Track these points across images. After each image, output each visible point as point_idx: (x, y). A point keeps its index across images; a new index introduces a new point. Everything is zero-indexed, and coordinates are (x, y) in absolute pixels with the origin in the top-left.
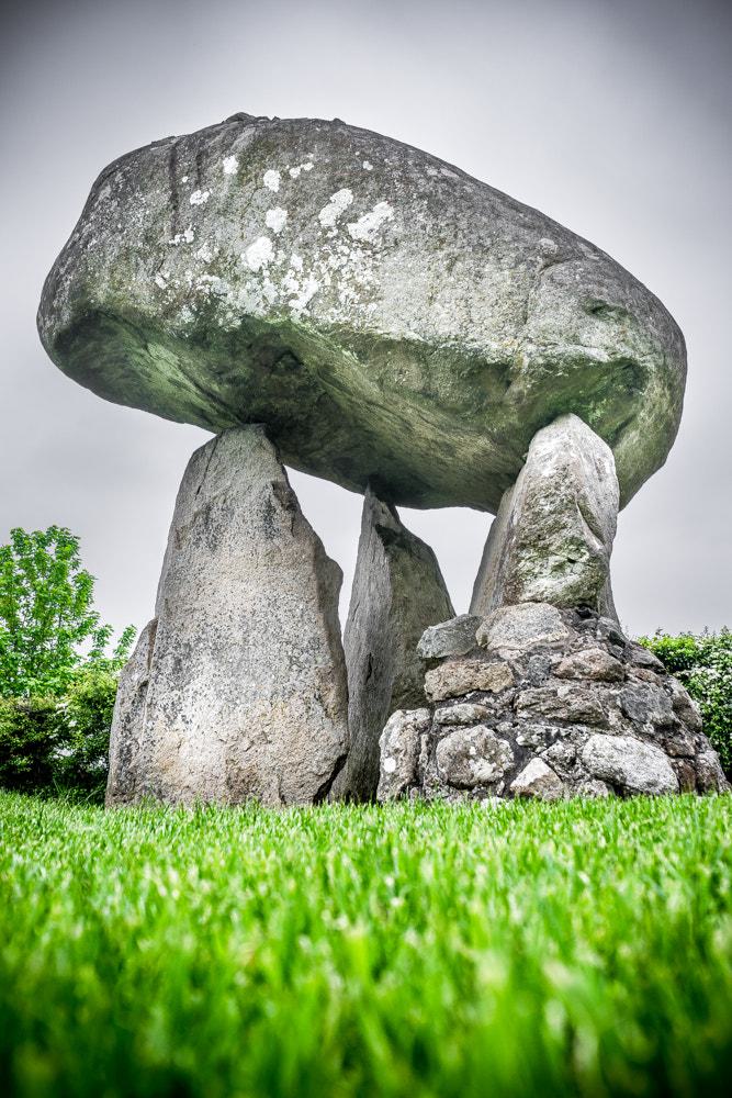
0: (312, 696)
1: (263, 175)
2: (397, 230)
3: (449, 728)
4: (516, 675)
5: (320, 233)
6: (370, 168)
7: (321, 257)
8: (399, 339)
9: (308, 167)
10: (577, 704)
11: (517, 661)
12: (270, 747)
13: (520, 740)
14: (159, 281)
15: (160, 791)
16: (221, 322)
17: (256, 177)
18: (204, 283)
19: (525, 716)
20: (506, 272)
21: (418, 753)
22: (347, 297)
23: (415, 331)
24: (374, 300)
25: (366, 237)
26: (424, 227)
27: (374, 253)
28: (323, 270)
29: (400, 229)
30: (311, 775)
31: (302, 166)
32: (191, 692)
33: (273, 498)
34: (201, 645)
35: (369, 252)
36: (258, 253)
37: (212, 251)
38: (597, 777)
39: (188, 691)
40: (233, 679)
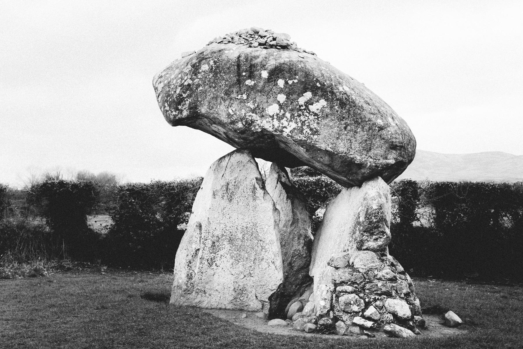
1: (278, 80)
2: (328, 110)
3: (343, 293)
4: (364, 277)
5: (298, 107)
7: (298, 116)
8: (324, 149)
9: (296, 81)
10: (384, 289)
11: (365, 273)
12: (252, 278)
13: (367, 300)
15: (205, 291)
16: (253, 129)
17: (275, 80)
18: (249, 116)
19: (368, 292)
20: (365, 132)
21: (332, 300)
22: (306, 132)
23: (330, 148)
24: (317, 135)
26: (337, 111)
27: (318, 118)
28: (298, 121)
29: (329, 111)
30: (269, 290)
31: (293, 80)
33: (256, 184)
34: (224, 237)
35: (316, 117)
36: (273, 109)
37: (254, 105)
38: (389, 313)
39: (218, 254)
40: (237, 252)
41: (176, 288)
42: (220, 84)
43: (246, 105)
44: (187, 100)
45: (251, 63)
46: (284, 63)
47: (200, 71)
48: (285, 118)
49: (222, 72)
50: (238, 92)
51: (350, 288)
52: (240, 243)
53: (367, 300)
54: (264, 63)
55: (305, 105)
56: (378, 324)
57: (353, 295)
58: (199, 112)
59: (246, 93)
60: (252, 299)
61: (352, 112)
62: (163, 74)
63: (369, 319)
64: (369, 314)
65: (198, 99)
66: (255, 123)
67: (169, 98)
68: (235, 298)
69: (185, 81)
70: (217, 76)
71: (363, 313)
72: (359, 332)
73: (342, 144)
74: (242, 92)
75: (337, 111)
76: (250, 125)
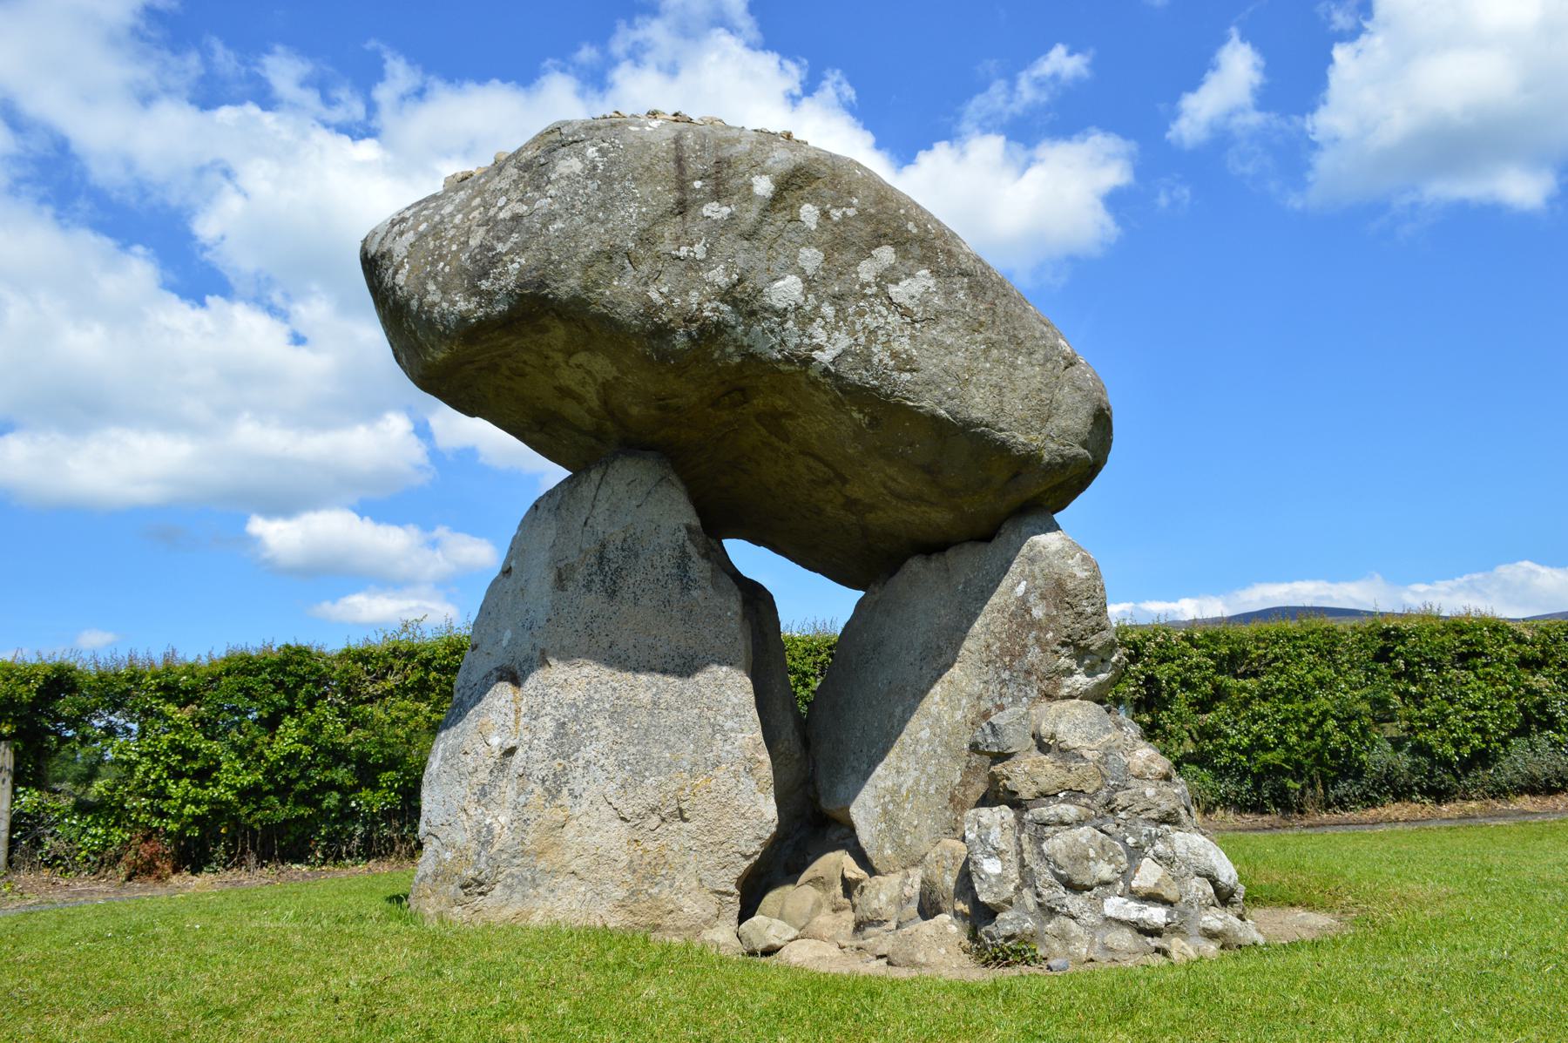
0: (742, 769)
1: (800, 207)
3: (1053, 829)
4: (1103, 776)
5: (857, 287)
6: (915, 231)
7: (856, 313)
9: (851, 212)
12: (686, 825)
13: (1131, 841)
14: (654, 296)
16: (716, 355)
18: (714, 310)
19: (1125, 817)
21: (1021, 852)
23: (946, 409)
25: (907, 302)
26: (964, 306)
27: (914, 322)
28: (858, 327)
29: (942, 303)
30: (738, 855)
31: (844, 209)
32: (581, 762)
34: (595, 706)
35: (908, 320)
37: (730, 276)
39: (576, 760)
41: (429, 880)
42: (623, 213)
43: (705, 276)
44: (512, 262)
45: (719, 154)
46: (817, 159)
47: (553, 177)
48: (819, 320)
49: (629, 177)
50: (678, 238)
51: (1070, 811)
52: (646, 720)
53: (1131, 841)
54: (758, 157)
55: (878, 285)
56: (1183, 914)
57: (1085, 832)
58: (551, 296)
59: (704, 240)
60: (687, 889)
61: (1000, 310)
62: (408, 214)
63: (1152, 898)
64: (1152, 885)
65: (550, 255)
66: (725, 335)
67: (442, 264)
68: (633, 892)
69: (501, 209)
70: (613, 189)
71: (1127, 884)
72: (1133, 947)
73: (977, 400)
74: (693, 236)
75: (964, 306)
76: (712, 339)
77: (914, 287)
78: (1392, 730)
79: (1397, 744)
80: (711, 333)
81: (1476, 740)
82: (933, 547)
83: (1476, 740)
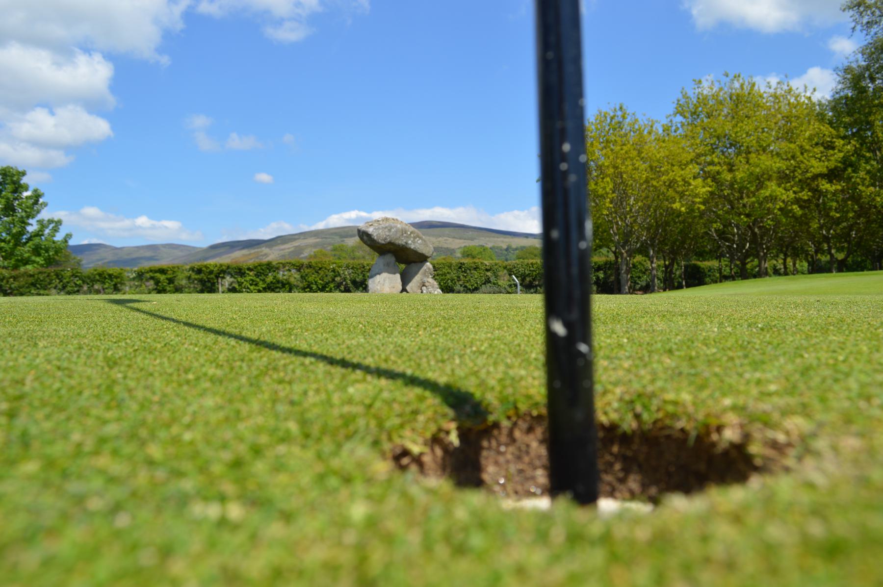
77: (420, 241)
78: (461, 283)
79: (461, 285)
80: (403, 245)
81: (476, 285)
82: (415, 262)
83: (476, 285)
